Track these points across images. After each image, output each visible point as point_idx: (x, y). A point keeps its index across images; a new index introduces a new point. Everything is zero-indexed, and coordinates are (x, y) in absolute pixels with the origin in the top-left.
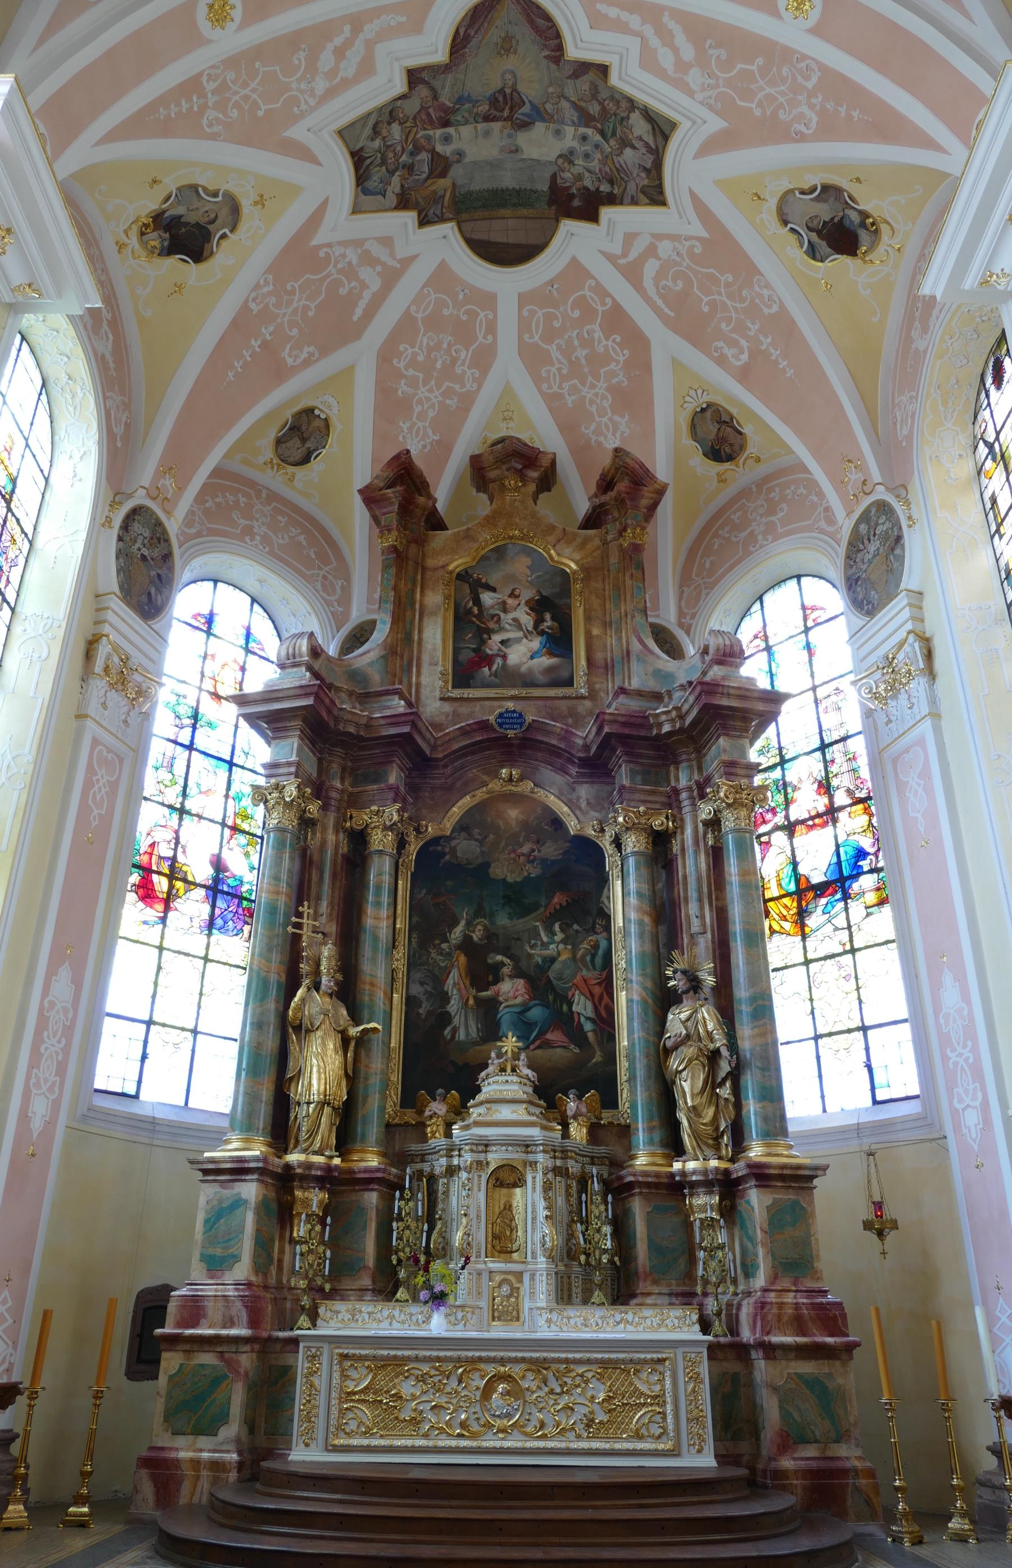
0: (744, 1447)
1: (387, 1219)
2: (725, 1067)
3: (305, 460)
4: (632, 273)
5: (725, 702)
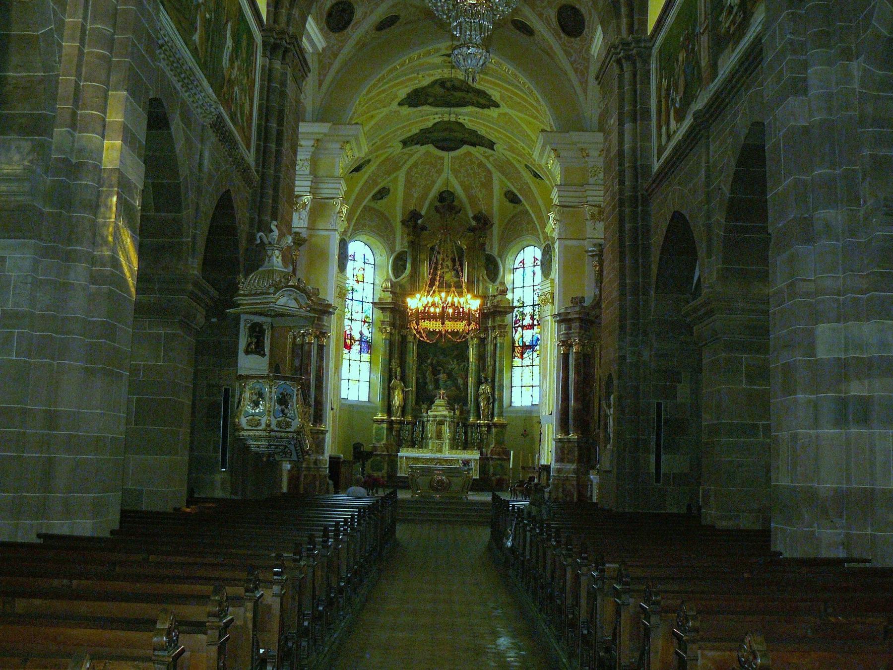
3: (382, 198)
4: (487, 158)
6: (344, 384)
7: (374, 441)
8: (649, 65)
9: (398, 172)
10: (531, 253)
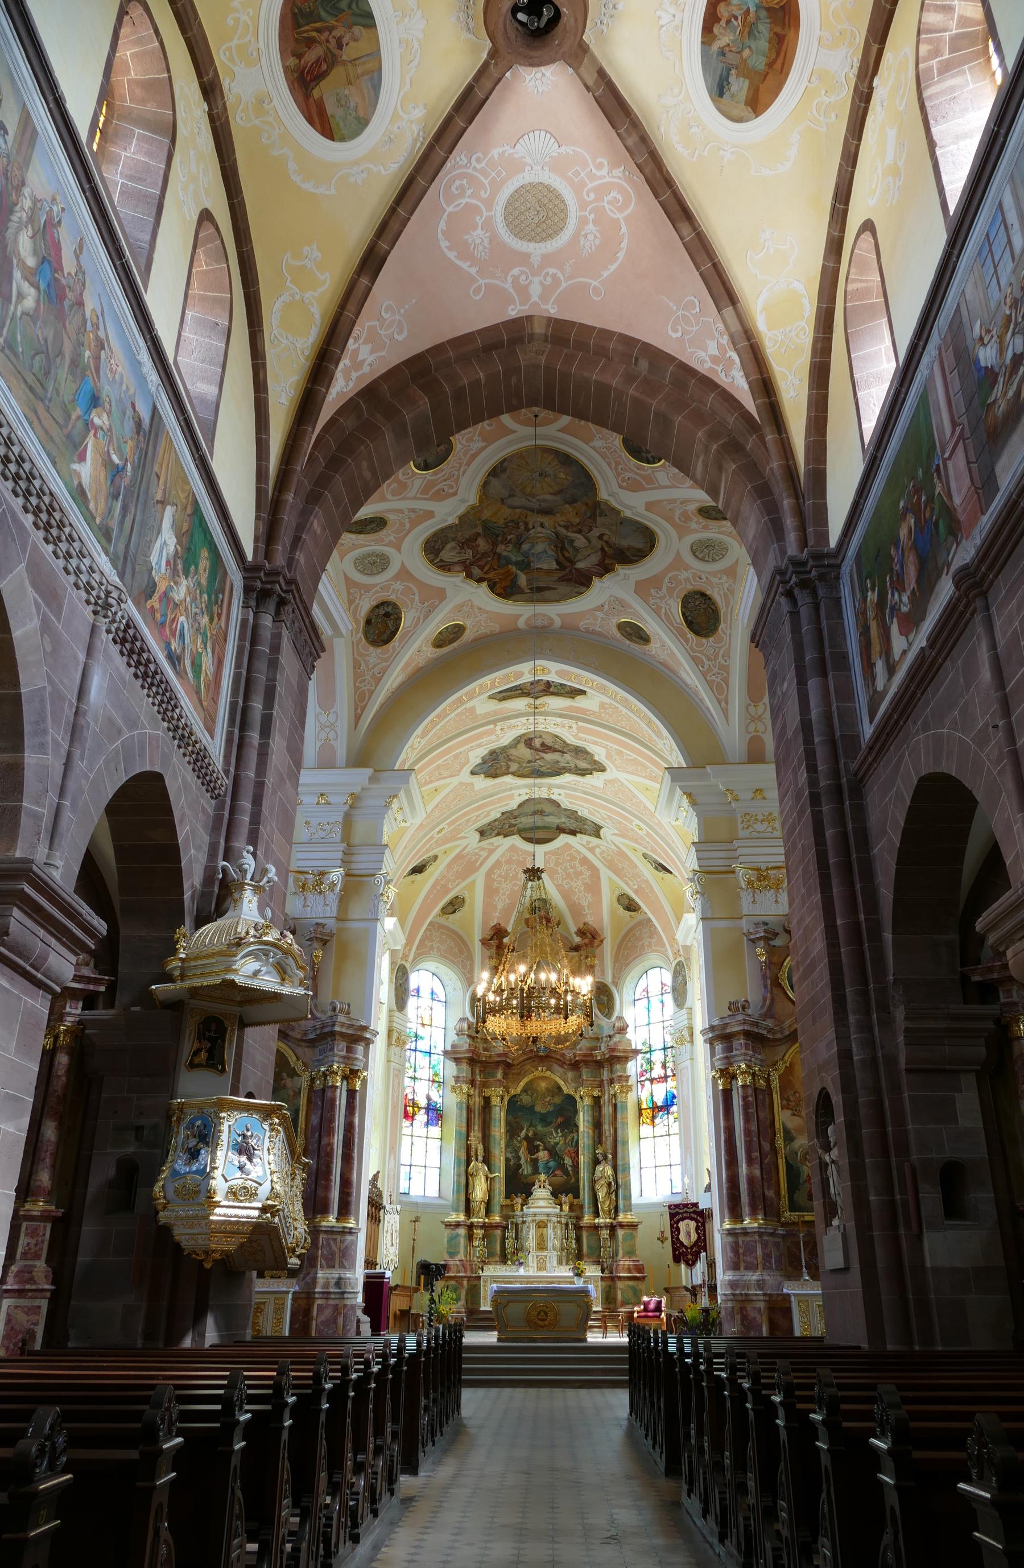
0: (612, 1306)
1: (504, 1239)
2: (613, 1188)
3: (454, 912)
4: (592, 850)
5: (618, 1054)
6: (404, 1171)
7: (447, 1257)
8: (838, 591)
9: (477, 873)
10: (658, 978)
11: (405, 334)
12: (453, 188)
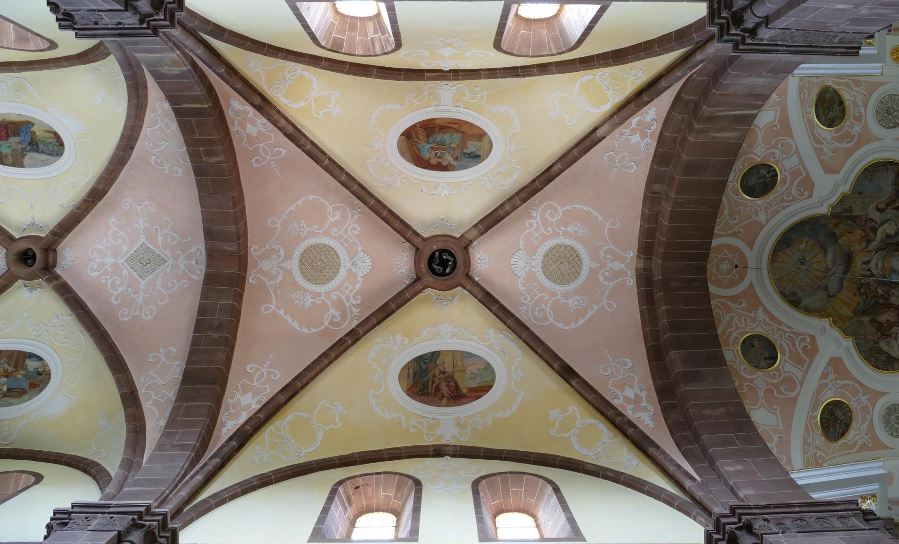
11: (628, 360)
12: (539, 316)
